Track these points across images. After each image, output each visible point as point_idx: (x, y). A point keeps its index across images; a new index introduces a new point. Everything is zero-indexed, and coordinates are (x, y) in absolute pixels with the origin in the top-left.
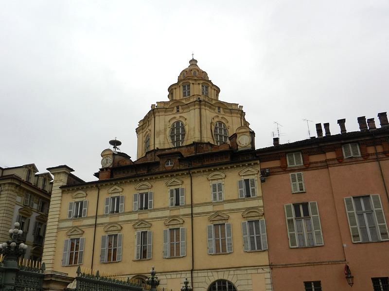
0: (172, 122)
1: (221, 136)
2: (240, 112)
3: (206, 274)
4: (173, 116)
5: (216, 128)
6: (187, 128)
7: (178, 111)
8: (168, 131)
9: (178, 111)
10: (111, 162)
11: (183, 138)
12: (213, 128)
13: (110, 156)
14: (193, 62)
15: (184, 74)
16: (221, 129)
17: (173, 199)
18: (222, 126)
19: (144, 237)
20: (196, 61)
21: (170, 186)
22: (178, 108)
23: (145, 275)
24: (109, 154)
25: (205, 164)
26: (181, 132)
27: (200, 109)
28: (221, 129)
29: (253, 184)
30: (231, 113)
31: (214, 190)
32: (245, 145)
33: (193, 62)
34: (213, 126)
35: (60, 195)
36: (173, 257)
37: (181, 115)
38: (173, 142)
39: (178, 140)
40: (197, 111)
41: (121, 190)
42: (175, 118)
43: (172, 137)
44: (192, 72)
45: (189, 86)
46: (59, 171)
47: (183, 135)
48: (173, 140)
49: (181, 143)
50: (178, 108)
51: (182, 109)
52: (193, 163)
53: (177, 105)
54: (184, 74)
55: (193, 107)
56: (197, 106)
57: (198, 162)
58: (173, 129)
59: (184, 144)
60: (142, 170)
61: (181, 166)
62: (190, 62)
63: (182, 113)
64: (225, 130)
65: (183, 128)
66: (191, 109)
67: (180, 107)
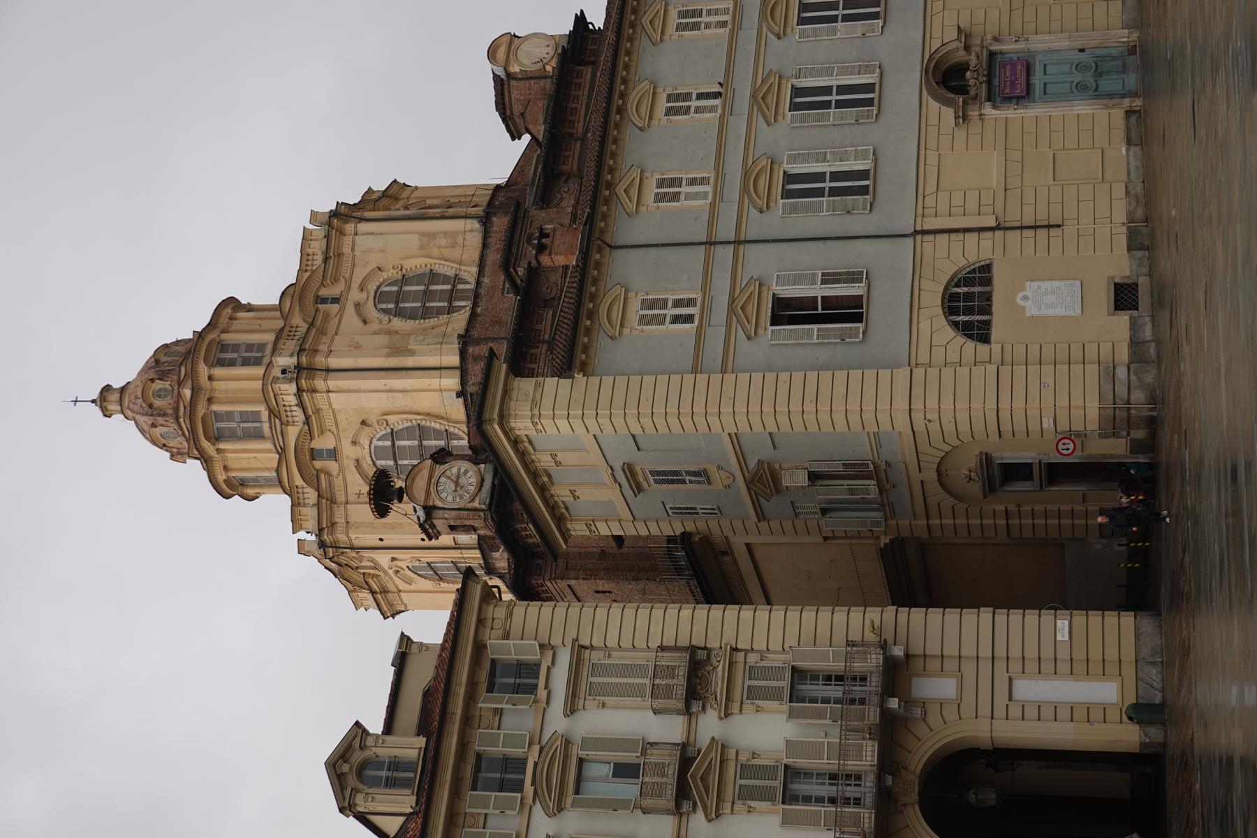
0: (371, 311)
4: (350, 310)
6: (416, 264)
7: (335, 300)
8: (397, 323)
9: (335, 300)
11: (446, 279)
13: (437, 473)
14: (107, 399)
15: (159, 394)
17: (706, 24)
19: (808, 100)
20: (107, 389)
21: (663, 33)
22: (324, 301)
23: (927, 57)
25: (580, 131)
26: (422, 288)
27: (362, 220)
30: (397, 199)
33: (107, 399)
35: (594, 381)
36: (882, 14)
38: (451, 310)
39: (451, 296)
40: (363, 227)
41: (636, 174)
42: (357, 306)
43: (426, 313)
44: (164, 359)
45: (224, 347)
46: (501, 386)
47: (433, 277)
48: (439, 311)
49: (460, 287)
50: (324, 301)
51: (335, 280)
52: (566, 168)
53: (310, 298)
54: (159, 394)
55: (347, 241)
56: (349, 227)
57: (567, 153)
58: (399, 313)
59: (470, 273)
60: (539, 327)
61: (564, 204)
62: (107, 414)
65: (405, 280)
66: (346, 250)
67: (324, 292)
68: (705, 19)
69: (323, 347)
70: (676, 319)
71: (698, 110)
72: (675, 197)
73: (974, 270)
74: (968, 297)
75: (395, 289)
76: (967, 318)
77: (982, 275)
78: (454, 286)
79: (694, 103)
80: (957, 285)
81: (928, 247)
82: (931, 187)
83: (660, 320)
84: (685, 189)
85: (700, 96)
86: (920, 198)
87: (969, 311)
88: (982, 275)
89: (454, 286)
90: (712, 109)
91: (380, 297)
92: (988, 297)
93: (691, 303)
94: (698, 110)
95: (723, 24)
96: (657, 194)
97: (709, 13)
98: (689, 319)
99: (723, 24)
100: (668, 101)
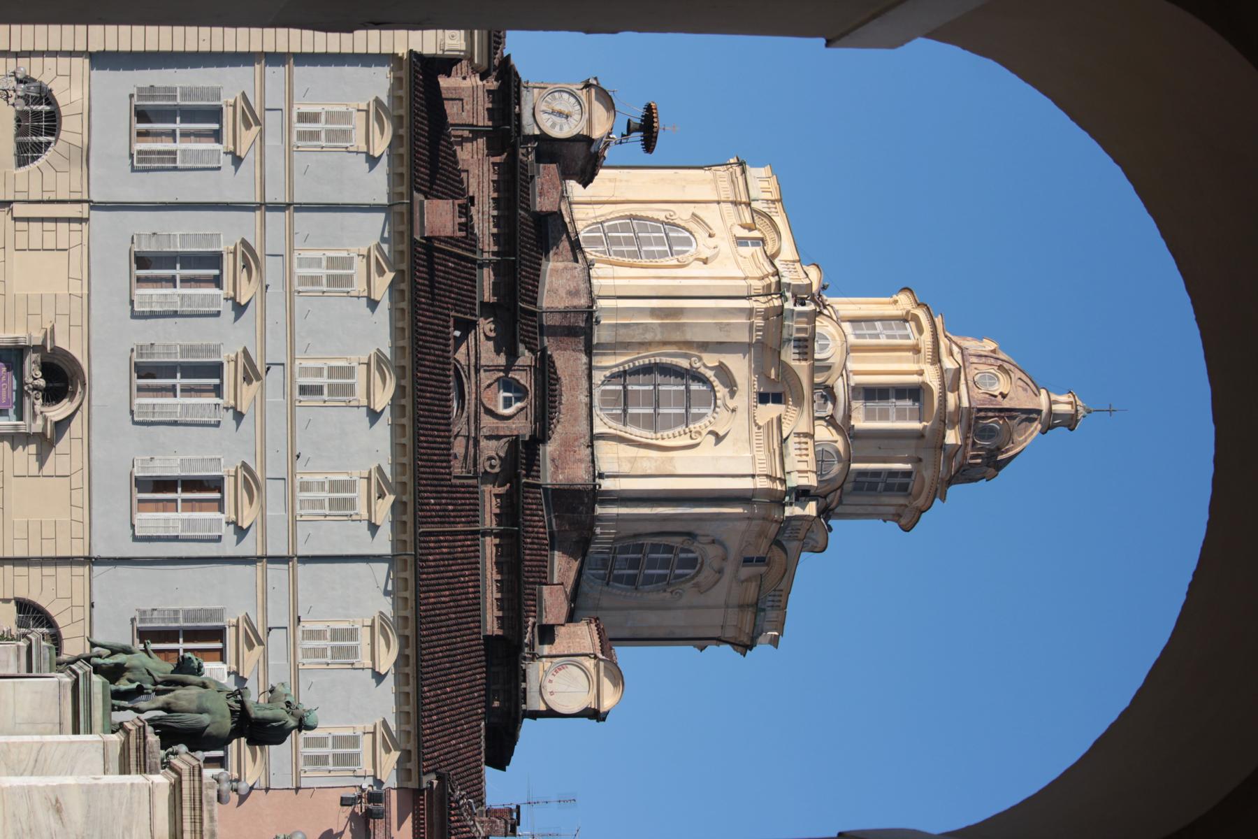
1: (635, 564)
2: (746, 640)
3: (78, 600)
5: (669, 549)
9: (763, 398)
10: (556, 133)
11: (636, 420)
12: (676, 541)
13: (584, 123)
16: (666, 564)
18: (678, 568)
24: (590, 121)
28: (666, 564)
29: (342, 760)
31: (336, 635)
32: (549, 687)
34: (676, 541)
37: (742, 415)
47: (651, 423)
63: (752, 419)
64: (662, 578)
68: (325, 495)
69: (759, 322)
70: (314, 118)
71: (319, 372)
72: (332, 262)
73: (34, 159)
74: (37, 131)
75: (694, 410)
76: (40, 108)
77: (26, 153)
78: (625, 411)
79: (323, 381)
80: (49, 143)
81: (76, 185)
82: (75, 252)
83: (331, 117)
84: (322, 272)
85: (317, 390)
86: (85, 242)
87: (37, 115)
88: (26, 153)
89: (625, 411)
90: (305, 371)
91: (711, 399)
92: (21, 130)
93: (303, 135)
94: (319, 372)
95: (306, 487)
96: (350, 267)
97: (320, 503)
98: (303, 117)
99: (306, 487)
100: (352, 386)
